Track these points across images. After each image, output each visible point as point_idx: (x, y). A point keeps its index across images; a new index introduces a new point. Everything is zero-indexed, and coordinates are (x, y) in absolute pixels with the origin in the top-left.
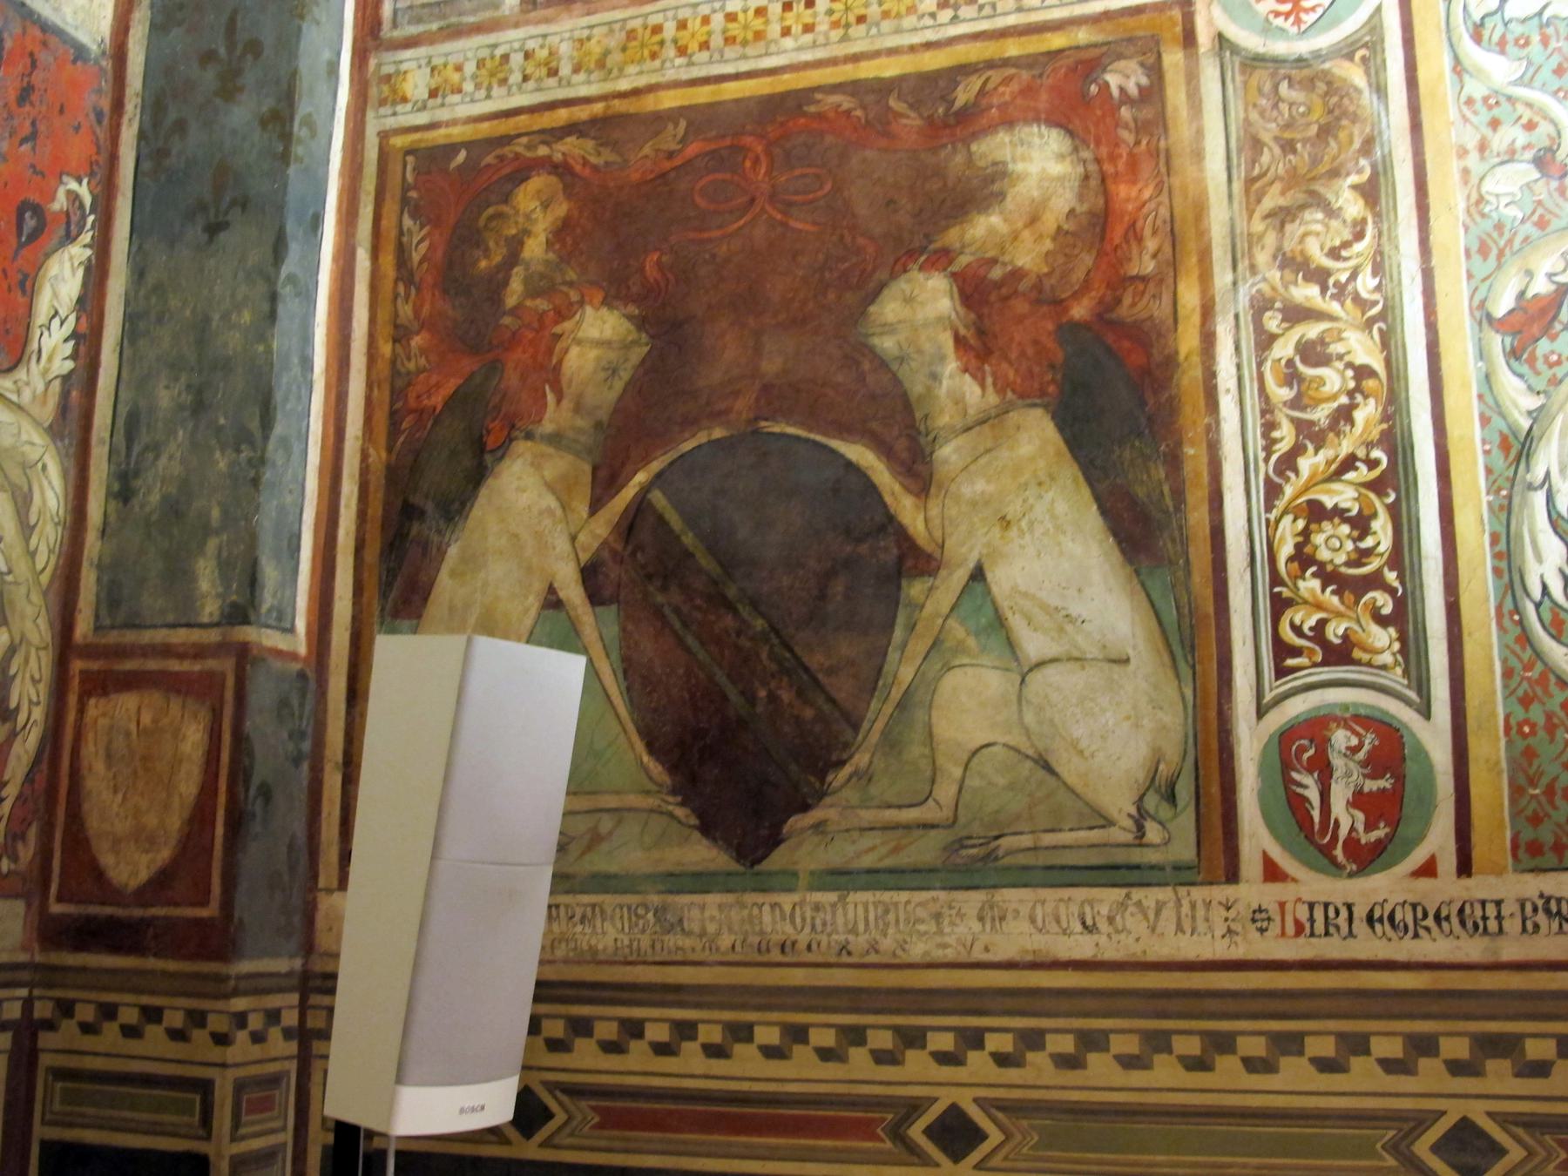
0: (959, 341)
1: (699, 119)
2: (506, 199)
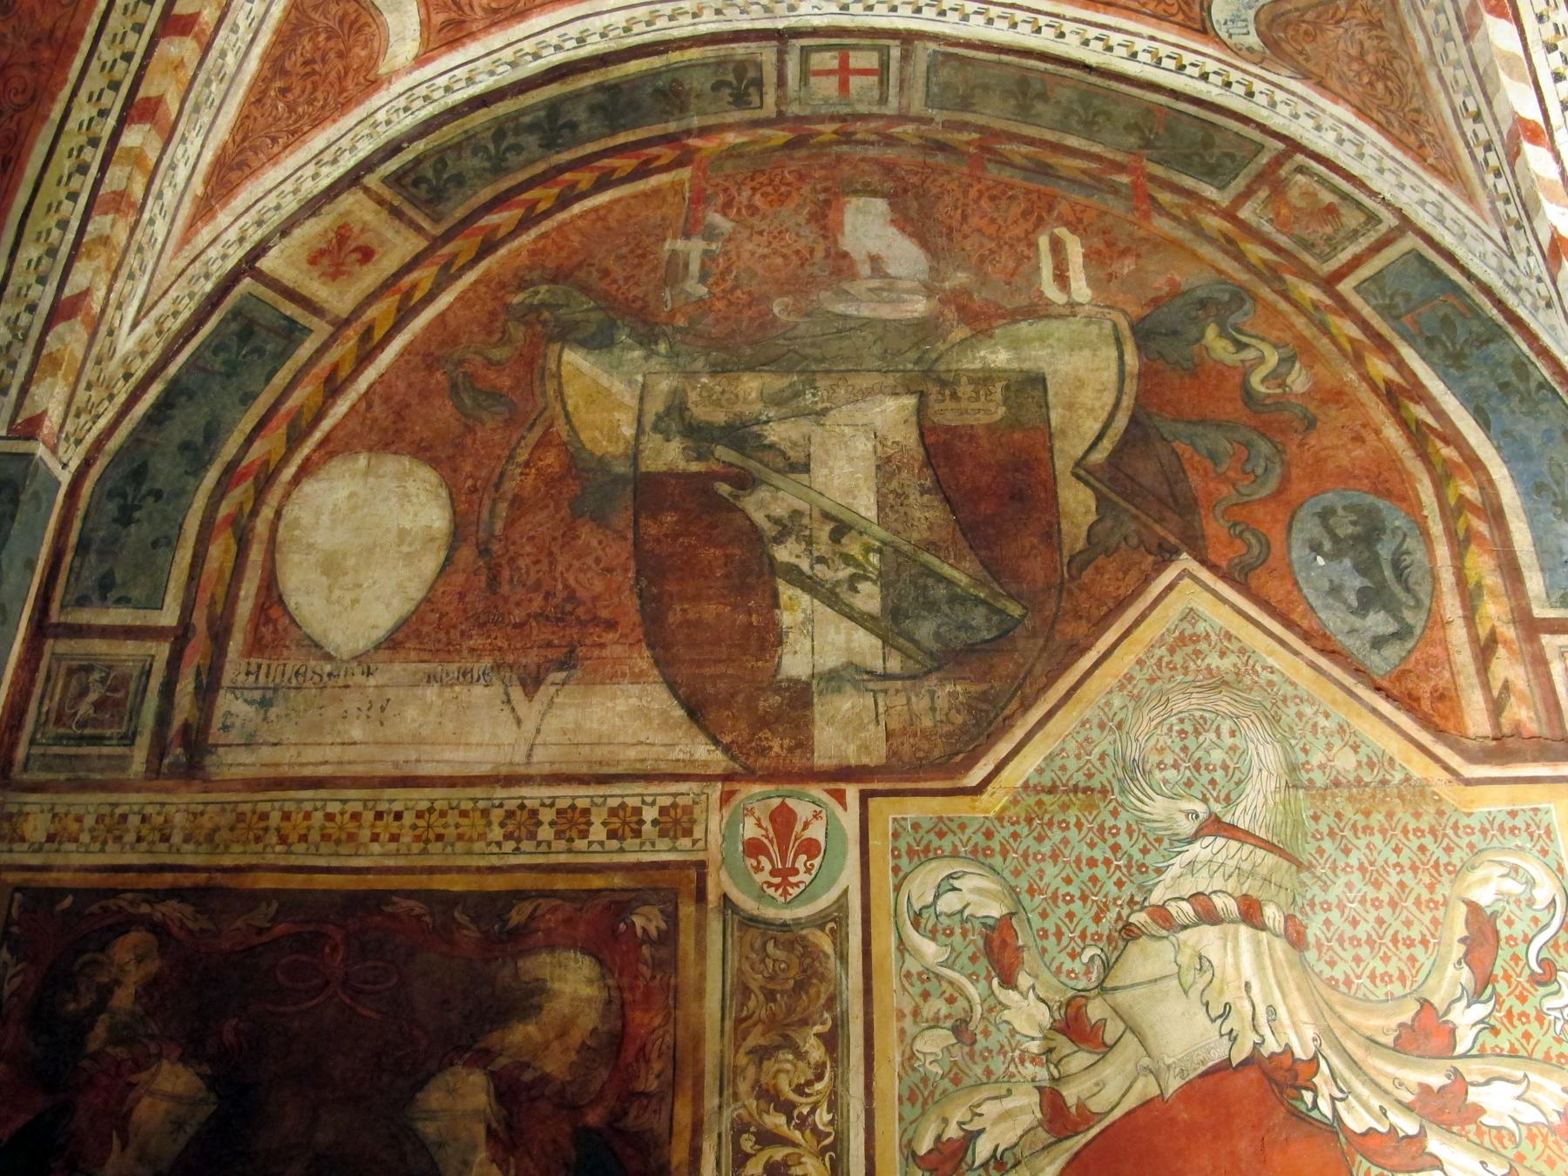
0: (490, 1132)
1: (290, 902)
2: (103, 949)
